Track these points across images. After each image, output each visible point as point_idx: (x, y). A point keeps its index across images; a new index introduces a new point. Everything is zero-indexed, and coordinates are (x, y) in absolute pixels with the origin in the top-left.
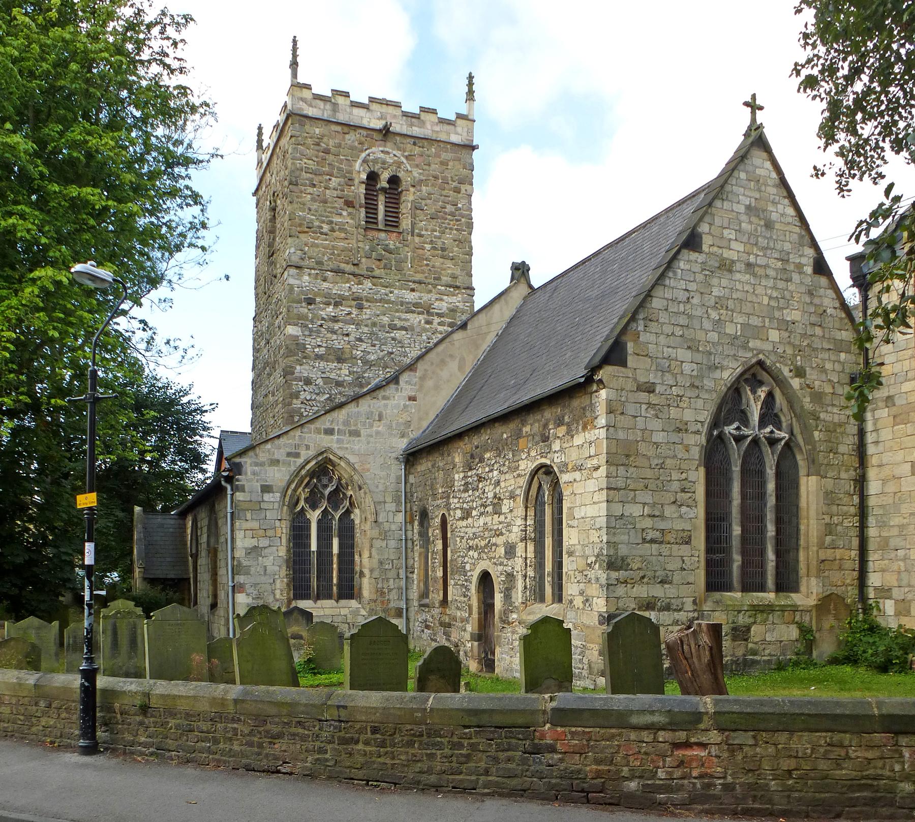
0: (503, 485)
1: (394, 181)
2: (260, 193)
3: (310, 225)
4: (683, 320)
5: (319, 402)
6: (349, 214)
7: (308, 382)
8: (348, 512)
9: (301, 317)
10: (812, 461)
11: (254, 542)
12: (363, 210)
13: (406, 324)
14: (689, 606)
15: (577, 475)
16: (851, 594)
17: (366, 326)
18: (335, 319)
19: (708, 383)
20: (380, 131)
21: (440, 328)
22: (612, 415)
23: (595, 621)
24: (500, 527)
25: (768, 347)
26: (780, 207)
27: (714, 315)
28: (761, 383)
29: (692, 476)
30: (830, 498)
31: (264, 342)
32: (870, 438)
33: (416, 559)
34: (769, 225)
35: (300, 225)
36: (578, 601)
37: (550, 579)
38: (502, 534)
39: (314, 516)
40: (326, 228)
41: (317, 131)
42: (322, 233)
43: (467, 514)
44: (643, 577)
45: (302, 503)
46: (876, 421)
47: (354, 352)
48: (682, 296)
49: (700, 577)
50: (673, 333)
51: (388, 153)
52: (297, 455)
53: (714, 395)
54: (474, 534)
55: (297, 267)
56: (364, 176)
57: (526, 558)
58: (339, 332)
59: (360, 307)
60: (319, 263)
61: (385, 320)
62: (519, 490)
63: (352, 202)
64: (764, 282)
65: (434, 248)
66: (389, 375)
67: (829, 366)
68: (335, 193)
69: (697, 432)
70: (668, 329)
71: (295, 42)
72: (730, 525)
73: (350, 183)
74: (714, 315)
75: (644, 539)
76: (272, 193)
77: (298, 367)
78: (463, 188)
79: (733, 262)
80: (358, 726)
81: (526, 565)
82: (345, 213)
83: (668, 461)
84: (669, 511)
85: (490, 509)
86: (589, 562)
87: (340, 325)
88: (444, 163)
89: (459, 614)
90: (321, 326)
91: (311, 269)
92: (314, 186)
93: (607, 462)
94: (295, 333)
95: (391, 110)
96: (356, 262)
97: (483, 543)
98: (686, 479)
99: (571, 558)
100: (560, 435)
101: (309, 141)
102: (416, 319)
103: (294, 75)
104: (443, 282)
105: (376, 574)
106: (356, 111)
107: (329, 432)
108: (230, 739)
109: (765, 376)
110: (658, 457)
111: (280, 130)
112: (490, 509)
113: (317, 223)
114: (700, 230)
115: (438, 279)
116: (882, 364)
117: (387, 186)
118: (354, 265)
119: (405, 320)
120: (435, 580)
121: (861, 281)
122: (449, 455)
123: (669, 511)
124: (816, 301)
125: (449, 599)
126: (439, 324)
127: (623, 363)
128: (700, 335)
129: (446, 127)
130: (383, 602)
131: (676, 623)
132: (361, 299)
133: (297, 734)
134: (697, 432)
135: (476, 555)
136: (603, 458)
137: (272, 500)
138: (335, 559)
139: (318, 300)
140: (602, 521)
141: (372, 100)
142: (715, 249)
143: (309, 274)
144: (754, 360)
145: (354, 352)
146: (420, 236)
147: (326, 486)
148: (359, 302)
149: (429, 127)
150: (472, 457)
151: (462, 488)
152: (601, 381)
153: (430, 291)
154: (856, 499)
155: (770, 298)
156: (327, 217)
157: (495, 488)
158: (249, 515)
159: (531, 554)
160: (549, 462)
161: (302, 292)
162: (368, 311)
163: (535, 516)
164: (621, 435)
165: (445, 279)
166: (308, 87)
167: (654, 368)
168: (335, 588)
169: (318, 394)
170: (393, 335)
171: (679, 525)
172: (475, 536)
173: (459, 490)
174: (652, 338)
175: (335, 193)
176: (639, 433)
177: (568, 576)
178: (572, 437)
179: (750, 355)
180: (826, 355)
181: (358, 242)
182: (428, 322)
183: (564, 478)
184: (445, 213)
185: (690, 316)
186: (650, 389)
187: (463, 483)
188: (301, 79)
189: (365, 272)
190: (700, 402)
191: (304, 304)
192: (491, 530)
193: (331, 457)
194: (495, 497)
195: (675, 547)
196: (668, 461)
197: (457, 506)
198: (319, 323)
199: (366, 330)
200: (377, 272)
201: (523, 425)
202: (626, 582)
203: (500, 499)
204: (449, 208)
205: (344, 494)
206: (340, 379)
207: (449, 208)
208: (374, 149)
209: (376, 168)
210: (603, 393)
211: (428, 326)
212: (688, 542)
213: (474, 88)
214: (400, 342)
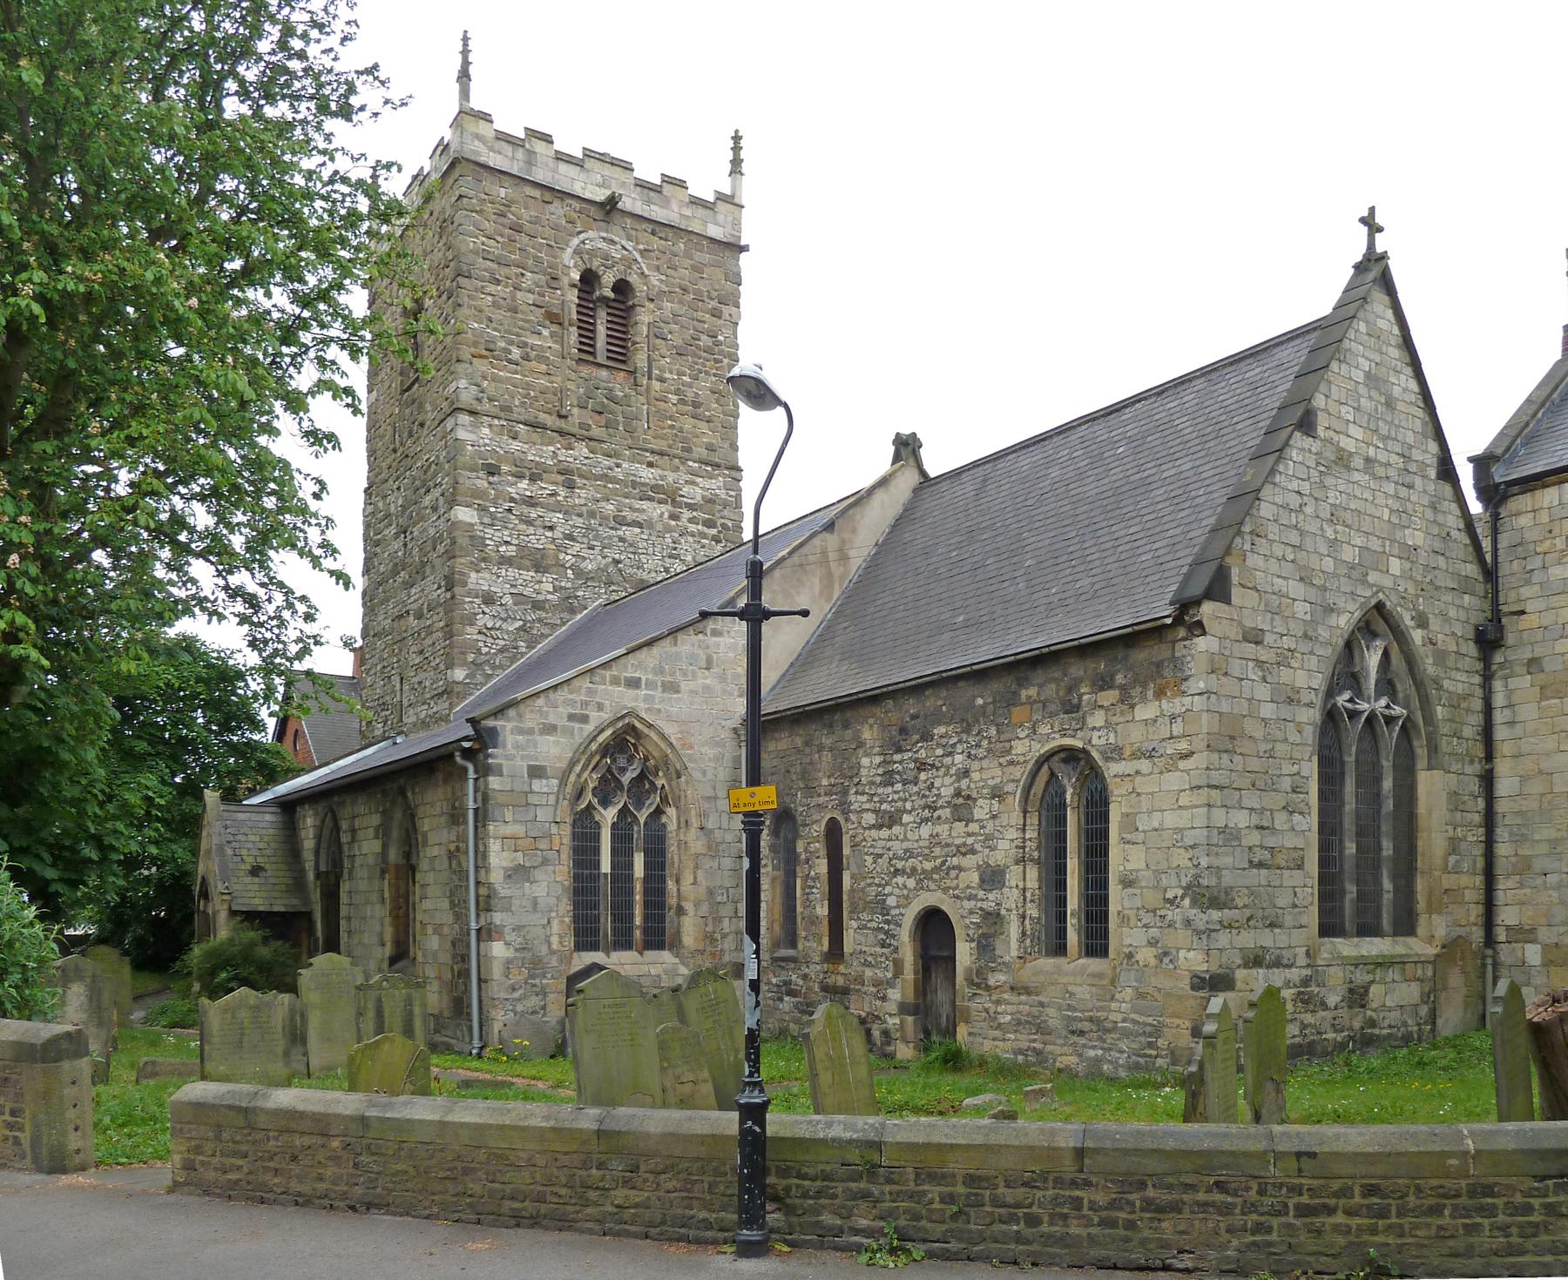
0: (975, 776)
1: (622, 287)
3: (492, 346)
4: (1294, 538)
5: (508, 632)
6: (552, 335)
7: (489, 599)
8: (658, 812)
12: (574, 330)
13: (641, 518)
14: (1302, 960)
15: (1144, 765)
17: (580, 515)
18: (531, 502)
19: (1323, 633)
20: (601, 205)
21: (692, 528)
23: (1185, 984)
24: (970, 841)
25: (1387, 582)
27: (1330, 533)
28: (1375, 635)
31: (393, 530)
32: (1499, 717)
35: (475, 344)
36: (1146, 955)
37: (1075, 921)
38: (973, 852)
40: (516, 353)
41: (503, 192)
44: (1249, 919)
46: (1509, 693)
47: (562, 556)
48: (1294, 501)
49: (1312, 917)
51: (613, 242)
52: (584, 719)
54: (906, 851)
55: (472, 413)
56: (576, 276)
57: (1024, 890)
58: (538, 523)
59: (571, 486)
61: (610, 508)
63: (557, 315)
65: (682, 402)
67: (1452, 613)
68: (531, 298)
69: (1310, 705)
70: (1278, 550)
72: (1341, 841)
77: (473, 575)
78: (726, 310)
79: (1351, 454)
80: (1336, 1185)
82: (546, 333)
83: (1279, 746)
84: (1281, 820)
86: (1170, 895)
87: (540, 511)
88: (697, 269)
90: (510, 510)
92: (498, 282)
94: (468, 519)
96: (564, 412)
97: (928, 866)
99: (1130, 891)
100: (1106, 704)
101: (489, 208)
102: (656, 511)
103: (465, 94)
104: (695, 455)
106: (563, 168)
107: (634, 683)
108: (1065, 1217)
109: (1381, 626)
110: (1265, 740)
113: (502, 344)
115: (689, 450)
116: (1523, 612)
117: (612, 295)
118: (560, 416)
119: (637, 510)
120: (813, 921)
121: (1492, 494)
122: (846, 726)
123: (1281, 820)
124: (1440, 518)
126: (691, 520)
127: (1226, 599)
128: (1314, 562)
129: (701, 212)
133: (1213, 1204)
134: (1310, 705)
136: (1199, 743)
137: (545, 790)
139: (505, 468)
141: (588, 154)
145: (562, 556)
146: (662, 380)
147: (623, 770)
148: (567, 474)
149: (675, 207)
150: (903, 731)
151: (878, 779)
152: (1200, 624)
153: (676, 469)
154: (1481, 803)
155: (1392, 511)
156: (518, 335)
157: (958, 780)
158: (509, 816)
160: (1080, 744)
161: (481, 455)
162: (583, 493)
164: (1225, 707)
165: (699, 451)
166: (486, 117)
167: (1262, 607)
171: (1290, 841)
172: (909, 853)
173: (873, 783)
175: (531, 298)
176: (1245, 704)
178: (1132, 707)
179: (1368, 593)
180: (1448, 597)
181: (573, 381)
182: (673, 517)
183: (1112, 770)
184: (698, 347)
185: (1302, 533)
186: (1254, 637)
187: (880, 771)
188: (476, 103)
189: (575, 430)
190: (1314, 659)
191: (481, 474)
192: (948, 845)
193: (637, 724)
194: (958, 794)
196: (1279, 746)
197: (867, 806)
198: (507, 505)
199: (579, 521)
200: (596, 432)
201: (1021, 685)
202: (1230, 926)
203: (969, 797)
204: (705, 340)
205: (652, 784)
206: (540, 597)
207: (705, 340)
208: (591, 234)
209: (595, 264)
210: (1201, 643)
212: (1300, 867)
213: (743, 154)
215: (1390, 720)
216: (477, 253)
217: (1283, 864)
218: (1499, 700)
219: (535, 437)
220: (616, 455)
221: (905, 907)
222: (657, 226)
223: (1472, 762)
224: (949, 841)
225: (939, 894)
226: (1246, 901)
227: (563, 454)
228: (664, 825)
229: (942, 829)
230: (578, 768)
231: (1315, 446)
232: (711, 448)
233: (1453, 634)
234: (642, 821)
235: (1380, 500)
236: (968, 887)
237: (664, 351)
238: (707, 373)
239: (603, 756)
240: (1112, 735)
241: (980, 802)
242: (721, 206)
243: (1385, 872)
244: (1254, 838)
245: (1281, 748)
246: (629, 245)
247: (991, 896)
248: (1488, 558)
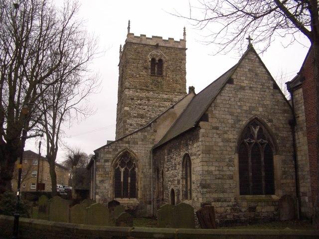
1: (160, 60)
4: (228, 106)
7: (131, 125)
8: (134, 169)
9: (129, 104)
10: (277, 150)
11: (102, 179)
16: (294, 194)
18: (140, 105)
20: (156, 46)
25: (258, 113)
26: (260, 69)
27: (239, 104)
28: (257, 125)
29: (233, 156)
30: (284, 162)
34: (256, 75)
36: (196, 199)
39: (122, 170)
48: (227, 98)
55: (128, 88)
59: (149, 100)
64: (256, 92)
68: (141, 65)
69: (235, 142)
70: (223, 109)
71: (129, 22)
74: (239, 104)
79: (245, 87)
84: (225, 169)
85: (173, 168)
95: (159, 39)
103: (129, 31)
104: (176, 91)
105: (142, 189)
106: (148, 40)
111: (125, 46)
112: (173, 168)
113: (135, 75)
114: (232, 77)
123: (225, 169)
124: (275, 97)
127: (208, 121)
128: (235, 111)
129: (177, 43)
134: (235, 142)
140: (201, 172)
141: (153, 37)
144: (254, 118)
146: (169, 77)
148: (148, 99)
159: (184, 183)
161: (130, 96)
164: (207, 144)
166: (133, 34)
171: (228, 173)
176: (214, 143)
183: (192, 158)
186: (217, 128)
188: (131, 32)
189: (150, 89)
195: (227, 180)
212: (232, 179)
215: (262, 144)
218: (297, 137)
219: (141, 92)
220: (159, 93)
222: (167, 48)
223: (290, 152)
226: (214, 187)
231: (233, 86)
232: (180, 89)
233: (282, 123)
235: (254, 95)
243: (263, 179)
244: (217, 173)
245: (225, 152)
246: (162, 52)
248: (291, 104)
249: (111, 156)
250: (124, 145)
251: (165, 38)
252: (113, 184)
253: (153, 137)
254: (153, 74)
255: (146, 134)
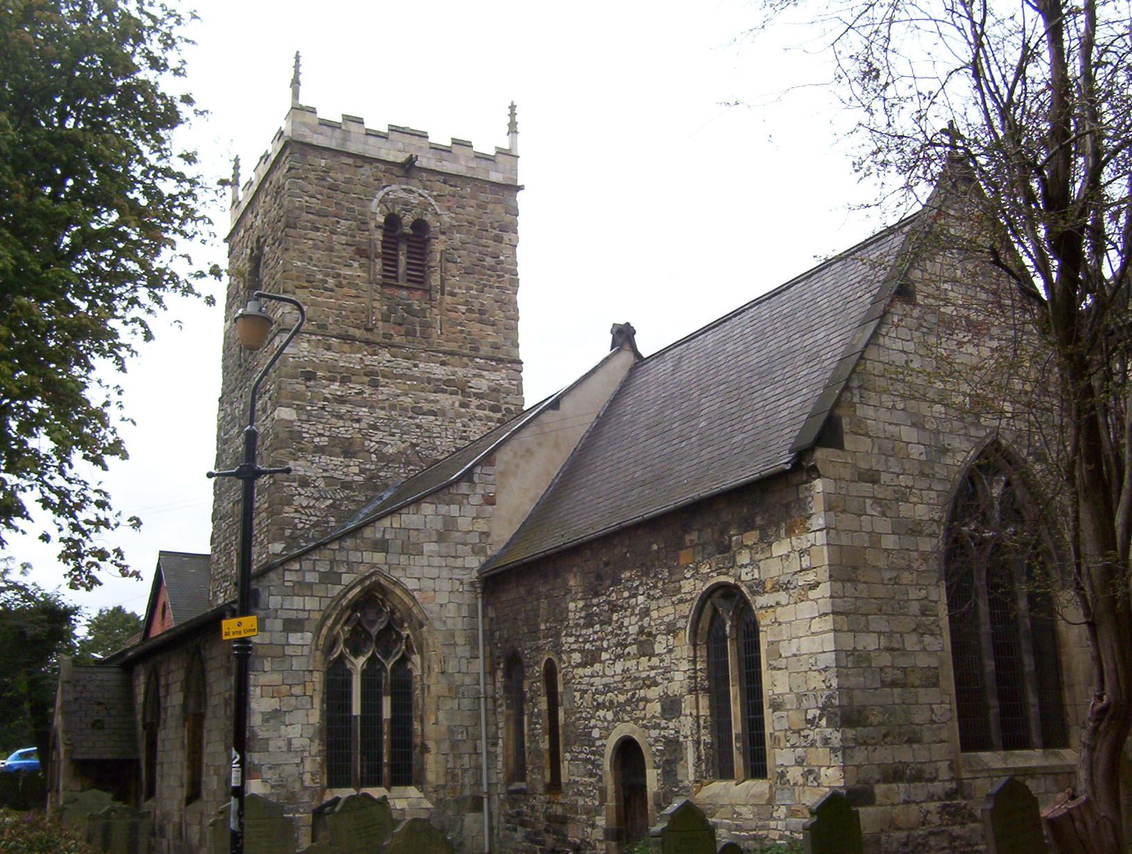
0: (654, 614)
2: (236, 239)
6: (361, 266)
8: (405, 659)
9: (296, 396)
12: (379, 262)
13: (434, 407)
17: (383, 409)
18: (341, 400)
20: (401, 165)
21: (480, 413)
22: (832, 513)
24: (652, 673)
33: (501, 725)
35: (298, 278)
36: (795, 774)
38: (656, 684)
40: (331, 282)
42: (326, 289)
43: (591, 658)
44: (885, 736)
45: (341, 647)
47: (367, 443)
49: (952, 732)
50: (894, 406)
51: (411, 192)
53: (949, 486)
54: (605, 685)
56: (381, 219)
57: (698, 717)
59: (375, 384)
60: (322, 327)
61: (408, 401)
62: (683, 621)
65: (470, 311)
66: (412, 474)
68: (344, 239)
73: (364, 227)
75: (883, 682)
76: (255, 239)
78: (506, 236)
81: (698, 726)
84: (911, 642)
85: (633, 649)
86: (810, 717)
89: (581, 802)
90: (323, 408)
91: (311, 334)
92: (318, 229)
93: (831, 576)
96: (370, 326)
97: (622, 698)
98: (926, 598)
99: (778, 713)
105: (445, 747)
106: (372, 140)
113: (320, 276)
115: (476, 349)
117: (411, 232)
118: (367, 330)
119: (432, 401)
120: (538, 753)
123: (911, 642)
125: (564, 780)
126: (478, 407)
129: (484, 163)
130: (454, 789)
131: (931, 798)
132: (376, 374)
135: (610, 715)
137: (300, 642)
138: (386, 728)
140: (829, 659)
142: (931, 301)
143: (309, 341)
145: (367, 443)
146: (453, 295)
147: (373, 623)
148: (373, 377)
149: (463, 162)
150: (599, 577)
151: (582, 621)
153: (466, 366)
156: (333, 268)
157: (641, 619)
158: (267, 666)
160: (732, 581)
162: (385, 390)
163: (708, 655)
165: (485, 350)
168: (386, 770)
169: (317, 499)
170: (417, 421)
171: (923, 661)
173: (577, 625)
174: (870, 412)
175: (344, 239)
177: (775, 740)
182: (463, 405)
184: (483, 267)
187: (583, 614)
189: (379, 339)
192: (636, 679)
193: (382, 581)
194: (641, 631)
195: (922, 691)
197: (574, 646)
198: (321, 404)
199: (382, 413)
202: (865, 743)
203: (650, 634)
204: (489, 261)
205: (399, 634)
206: (348, 479)
207: (489, 261)
208: (394, 187)
211: (463, 410)
212: (935, 685)
214: (426, 431)
216: (301, 208)
217: (917, 682)
219: (346, 347)
221: (606, 738)
222: (447, 177)
224: (637, 675)
225: (631, 724)
226: (879, 719)
227: (368, 360)
228: (410, 671)
229: (631, 664)
230: (329, 623)
232: (495, 347)
234: (389, 667)
236: (653, 717)
237: (455, 272)
238: (491, 287)
239: (354, 611)
240: (756, 571)
241: (659, 638)
242: (501, 158)
244: (886, 659)
245: (906, 577)
246: (425, 193)
247: (671, 725)
249: (311, 603)
250: (367, 556)
251: (441, 138)
252: (321, 730)
253: (481, 526)
254: (389, 279)
255: (454, 510)
